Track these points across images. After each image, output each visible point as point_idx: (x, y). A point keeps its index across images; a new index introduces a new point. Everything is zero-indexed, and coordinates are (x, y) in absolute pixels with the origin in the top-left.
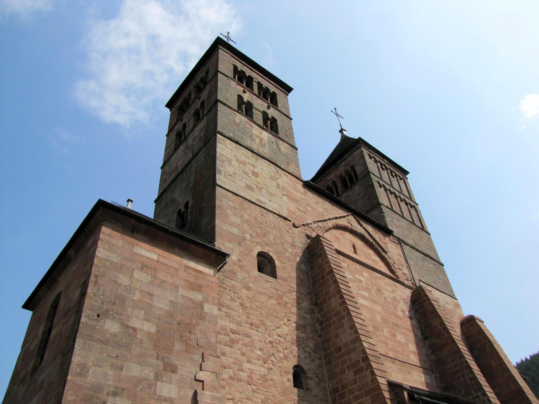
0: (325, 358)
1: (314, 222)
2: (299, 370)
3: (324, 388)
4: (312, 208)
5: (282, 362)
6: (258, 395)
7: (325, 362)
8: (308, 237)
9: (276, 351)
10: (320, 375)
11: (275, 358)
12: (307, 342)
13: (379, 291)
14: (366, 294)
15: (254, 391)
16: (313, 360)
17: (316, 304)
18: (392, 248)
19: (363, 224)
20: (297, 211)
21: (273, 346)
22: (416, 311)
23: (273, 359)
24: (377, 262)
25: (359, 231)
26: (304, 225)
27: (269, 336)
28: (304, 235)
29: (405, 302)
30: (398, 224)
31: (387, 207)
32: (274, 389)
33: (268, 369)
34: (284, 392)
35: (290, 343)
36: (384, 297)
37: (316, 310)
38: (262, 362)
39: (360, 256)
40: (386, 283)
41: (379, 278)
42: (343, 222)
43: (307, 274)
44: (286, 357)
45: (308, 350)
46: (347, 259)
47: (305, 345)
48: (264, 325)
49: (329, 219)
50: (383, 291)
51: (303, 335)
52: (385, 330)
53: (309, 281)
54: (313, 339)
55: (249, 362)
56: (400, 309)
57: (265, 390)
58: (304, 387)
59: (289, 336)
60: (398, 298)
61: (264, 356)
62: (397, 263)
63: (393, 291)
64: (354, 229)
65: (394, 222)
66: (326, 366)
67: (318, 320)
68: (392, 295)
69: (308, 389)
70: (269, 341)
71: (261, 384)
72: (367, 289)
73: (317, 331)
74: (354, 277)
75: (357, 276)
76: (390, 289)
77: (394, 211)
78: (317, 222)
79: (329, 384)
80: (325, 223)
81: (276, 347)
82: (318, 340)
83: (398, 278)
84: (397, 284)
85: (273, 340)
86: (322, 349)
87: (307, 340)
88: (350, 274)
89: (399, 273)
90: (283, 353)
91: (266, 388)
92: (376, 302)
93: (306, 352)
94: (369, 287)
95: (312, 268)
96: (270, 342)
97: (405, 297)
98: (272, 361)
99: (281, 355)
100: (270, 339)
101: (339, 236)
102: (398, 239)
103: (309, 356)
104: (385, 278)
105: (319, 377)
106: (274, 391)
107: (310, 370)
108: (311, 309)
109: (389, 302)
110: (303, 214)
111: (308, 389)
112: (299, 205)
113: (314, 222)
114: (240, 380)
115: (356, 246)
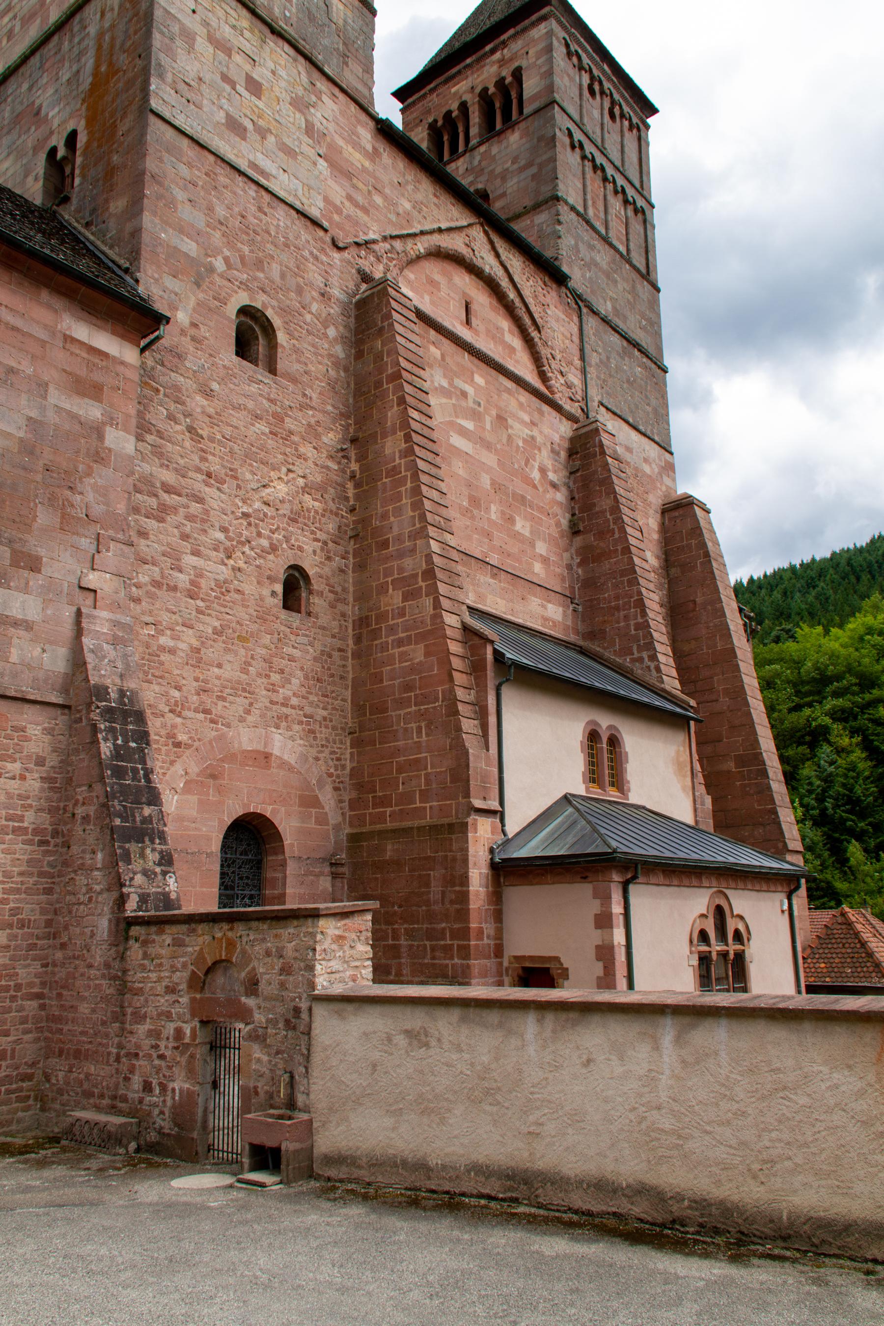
0: (354, 557)
1: (385, 239)
2: (297, 574)
3: (343, 615)
4: (385, 198)
5: (264, 558)
6: (207, 619)
8: (365, 277)
9: (254, 534)
11: (252, 549)
12: (323, 520)
13: (501, 420)
14: (469, 425)
15: (199, 611)
16: (329, 558)
17: (353, 441)
18: (557, 320)
19: (501, 251)
21: (250, 524)
22: (571, 473)
23: (246, 549)
24: (512, 350)
25: (487, 269)
26: (357, 244)
27: (244, 501)
28: (354, 271)
29: (553, 451)
30: (587, 259)
31: (573, 209)
32: (240, 609)
33: (234, 569)
34: (262, 617)
35: (286, 519)
36: (509, 436)
37: (352, 455)
38: (222, 555)
39: (477, 333)
40: (521, 405)
41: (508, 391)
42: (455, 243)
43: (346, 370)
44: (274, 548)
45: (319, 534)
46: (444, 340)
48: (236, 478)
49: (422, 233)
50: (510, 421)
51: (317, 504)
52: (493, 508)
53: (348, 384)
54: (337, 514)
55: (196, 553)
56: (536, 465)
57: (223, 610)
58: (303, 608)
59: (287, 506)
61: (228, 544)
62: (558, 357)
63: (533, 423)
64: (478, 262)
65: (578, 251)
66: (353, 572)
67: (353, 477)
68: (527, 431)
69: (309, 614)
70: (243, 513)
71: (216, 597)
72: (476, 416)
73: (347, 499)
74: (451, 384)
75: (459, 383)
76: (527, 418)
77: (588, 222)
78: (392, 237)
79: (354, 606)
80: (410, 243)
81: (257, 526)
82: (347, 518)
83: (552, 393)
84: (546, 408)
85: (250, 510)
87: (323, 516)
88: (445, 376)
89: (557, 383)
90: (269, 538)
91: (225, 607)
92: (488, 446)
94: (481, 409)
95: (359, 355)
96: (246, 515)
97: (556, 438)
98: (243, 553)
99: (265, 543)
100: (245, 509)
101: (437, 277)
102: (578, 297)
103: (322, 549)
104: (521, 390)
105: (335, 593)
106: (241, 613)
107: (321, 577)
108: (342, 450)
110: (360, 213)
111: (309, 614)
112: (354, 187)
113: (385, 239)
114: (175, 589)
115: (474, 307)
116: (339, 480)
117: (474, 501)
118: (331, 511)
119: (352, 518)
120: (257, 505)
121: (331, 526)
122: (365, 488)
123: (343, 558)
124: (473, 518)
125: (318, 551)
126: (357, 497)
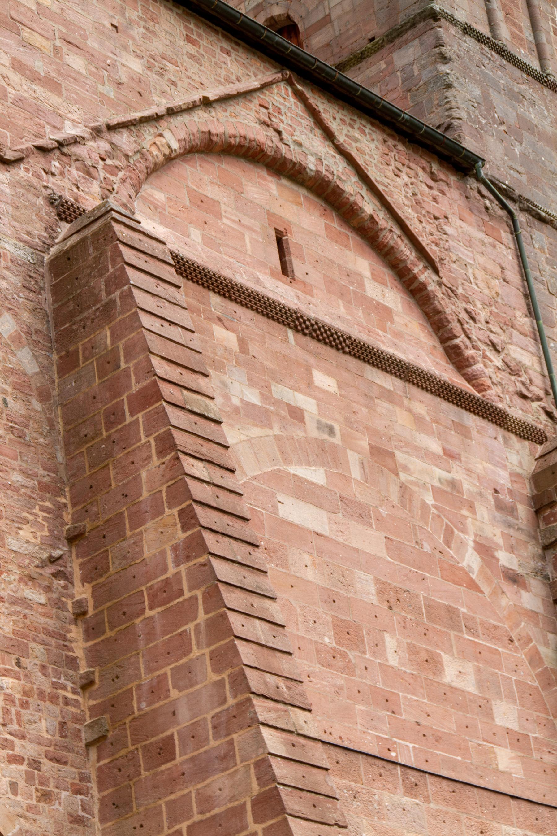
1: (97, 132)
4: (90, 56)
7: (102, 801)
8: (65, 211)
12: (26, 714)
13: (381, 456)
14: (316, 475)
16: (46, 796)
17: (74, 539)
18: (469, 243)
19: (334, 126)
20: (15, 77)
22: (546, 548)
24: (385, 313)
25: (311, 164)
26: (41, 149)
28: (40, 201)
29: (500, 506)
30: (512, 120)
31: (467, 30)
36: (403, 487)
37: (75, 567)
39: (307, 288)
40: (418, 420)
41: (388, 396)
42: (241, 123)
43: (44, 396)
45: (21, 748)
46: (241, 311)
47: (14, 727)
49: (171, 112)
50: (400, 456)
52: (390, 642)
53: (52, 426)
54: (53, 699)
56: (470, 541)
60: (466, 486)
62: (482, 315)
63: (449, 455)
64: (292, 153)
65: (491, 108)
66: (102, 820)
67: (80, 614)
68: (438, 472)
73: (72, 662)
74: (266, 397)
75: (283, 392)
76: (435, 447)
77: (501, 51)
78: (110, 128)
80: (148, 135)
82: (76, 704)
83: (481, 388)
84: (472, 421)
86: (88, 745)
87: (25, 705)
88: (252, 383)
89: (487, 366)
92: (362, 514)
93: (16, 759)
94: (337, 440)
95: (68, 364)
97: (503, 479)
101: (212, 191)
102: (503, 194)
103: (29, 778)
104: (415, 391)
108: (52, 560)
109: (424, 505)
110: (40, 91)
112: (27, 45)
113: (97, 132)
115: (293, 239)
116: (52, 624)
117: (348, 633)
118: (41, 694)
119: (87, 703)
121: (43, 725)
122: (109, 634)
123: (78, 792)
124: (349, 669)
125: (22, 784)
126: (94, 656)
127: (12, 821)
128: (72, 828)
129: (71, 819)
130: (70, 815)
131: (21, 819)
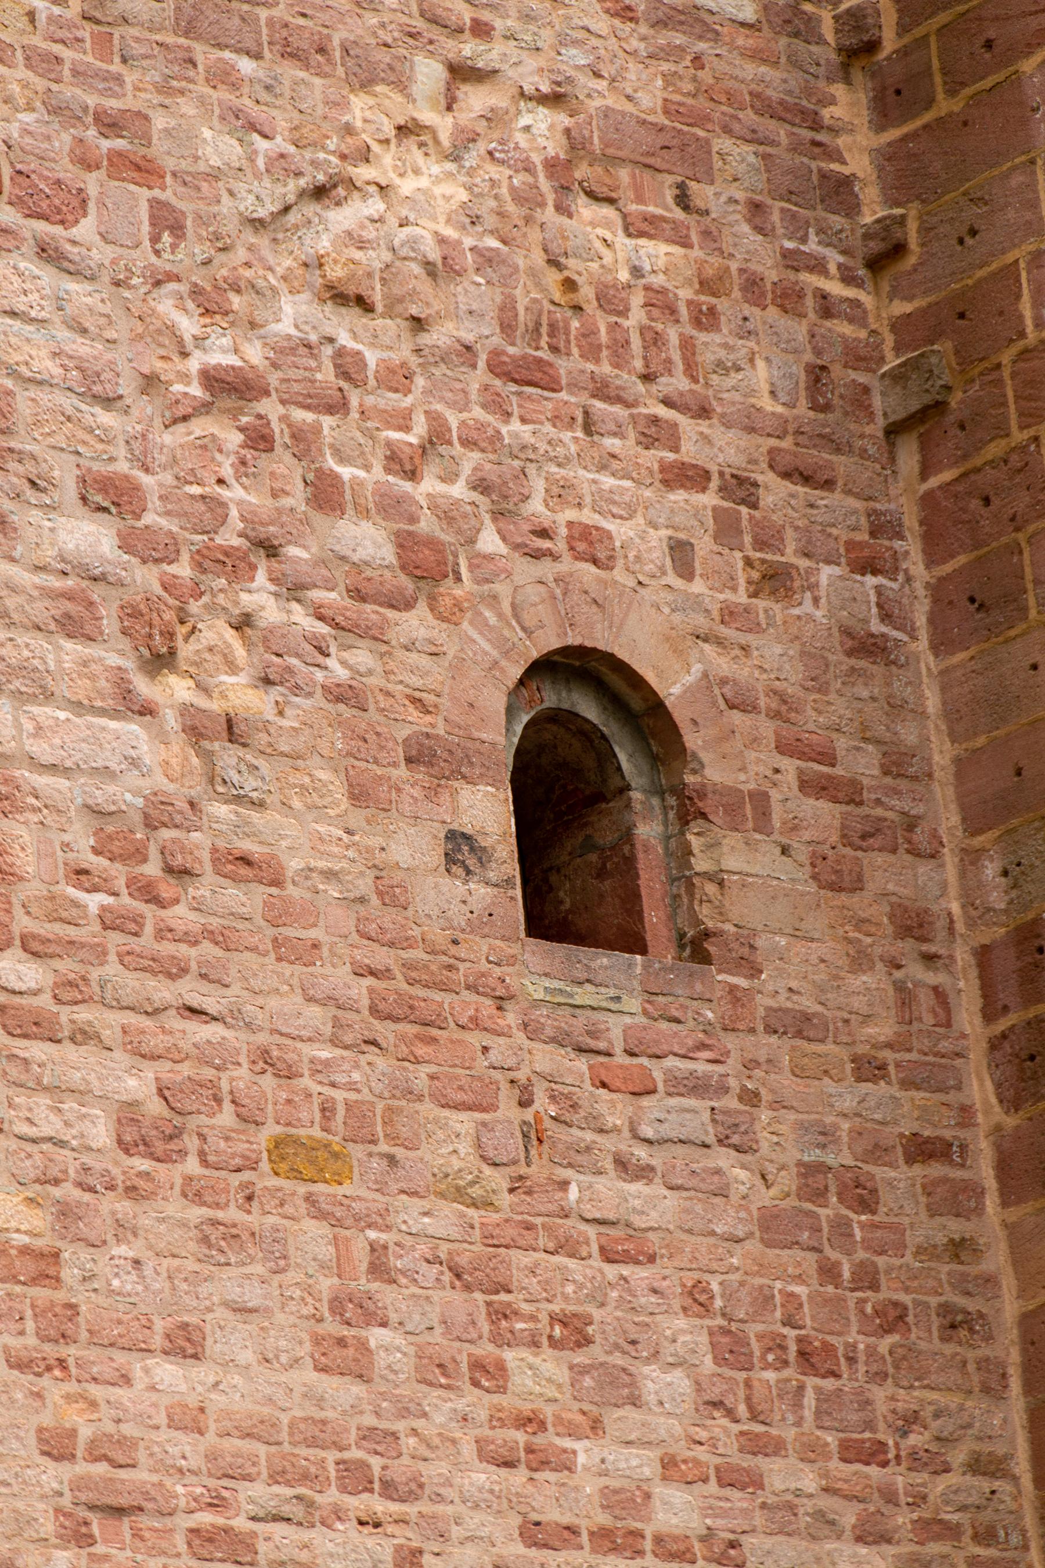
0: (935, 546)
2: (589, 709)
3: (913, 924)
5: (374, 635)
6: (74, 1063)
7: (937, 591)
9: (297, 499)
10: (863, 765)
11: (293, 590)
12: (711, 345)
16: (774, 581)
21: (260, 439)
23: (259, 596)
27: (210, 306)
32: (268, 971)
33: (196, 730)
34: (405, 1011)
35: (478, 377)
38: (115, 655)
44: (425, 567)
45: (698, 442)
47: (678, 383)
48: (145, 171)
51: (655, 252)
54: (788, 300)
57: (162, 991)
58: (654, 918)
59: (475, 292)
61: (146, 578)
66: (940, 645)
67: (858, 50)
69: (696, 948)
70: (211, 379)
71: (110, 921)
73: (839, 192)
79: (971, 858)
81: (303, 442)
82: (855, 313)
85: (255, 354)
86: (893, 431)
87: (706, 319)
90: (392, 506)
91: (175, 971)
93: (685, 476)
96: (229, 388)
98: (243, 623)
99: (368, 541)
100: (220, 353)
103: (726, 529)
105: (848, 793)
106: (280, 1001)
107: (740, 703)
111: (696, 948)
116: (775, 81)
118: (752, 286)
119: (882, 308)
120: (292, 314)
121: (761, 374)
122: (945, 105)
123: (867, 566)
125: (704, 545)
126: (902, 171)
127: (679, 652)
128: (853, 669)
129: (850, 643)
130: (847, 632)
131: (706, 646)
